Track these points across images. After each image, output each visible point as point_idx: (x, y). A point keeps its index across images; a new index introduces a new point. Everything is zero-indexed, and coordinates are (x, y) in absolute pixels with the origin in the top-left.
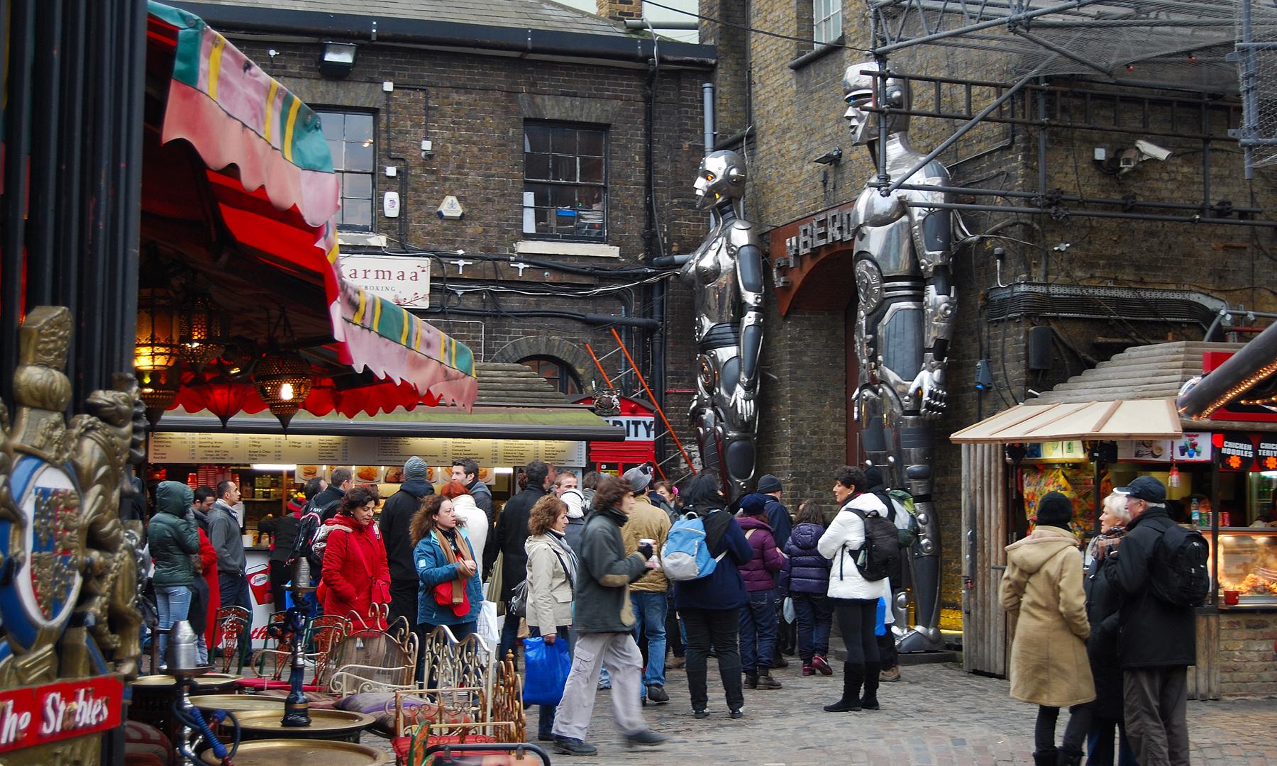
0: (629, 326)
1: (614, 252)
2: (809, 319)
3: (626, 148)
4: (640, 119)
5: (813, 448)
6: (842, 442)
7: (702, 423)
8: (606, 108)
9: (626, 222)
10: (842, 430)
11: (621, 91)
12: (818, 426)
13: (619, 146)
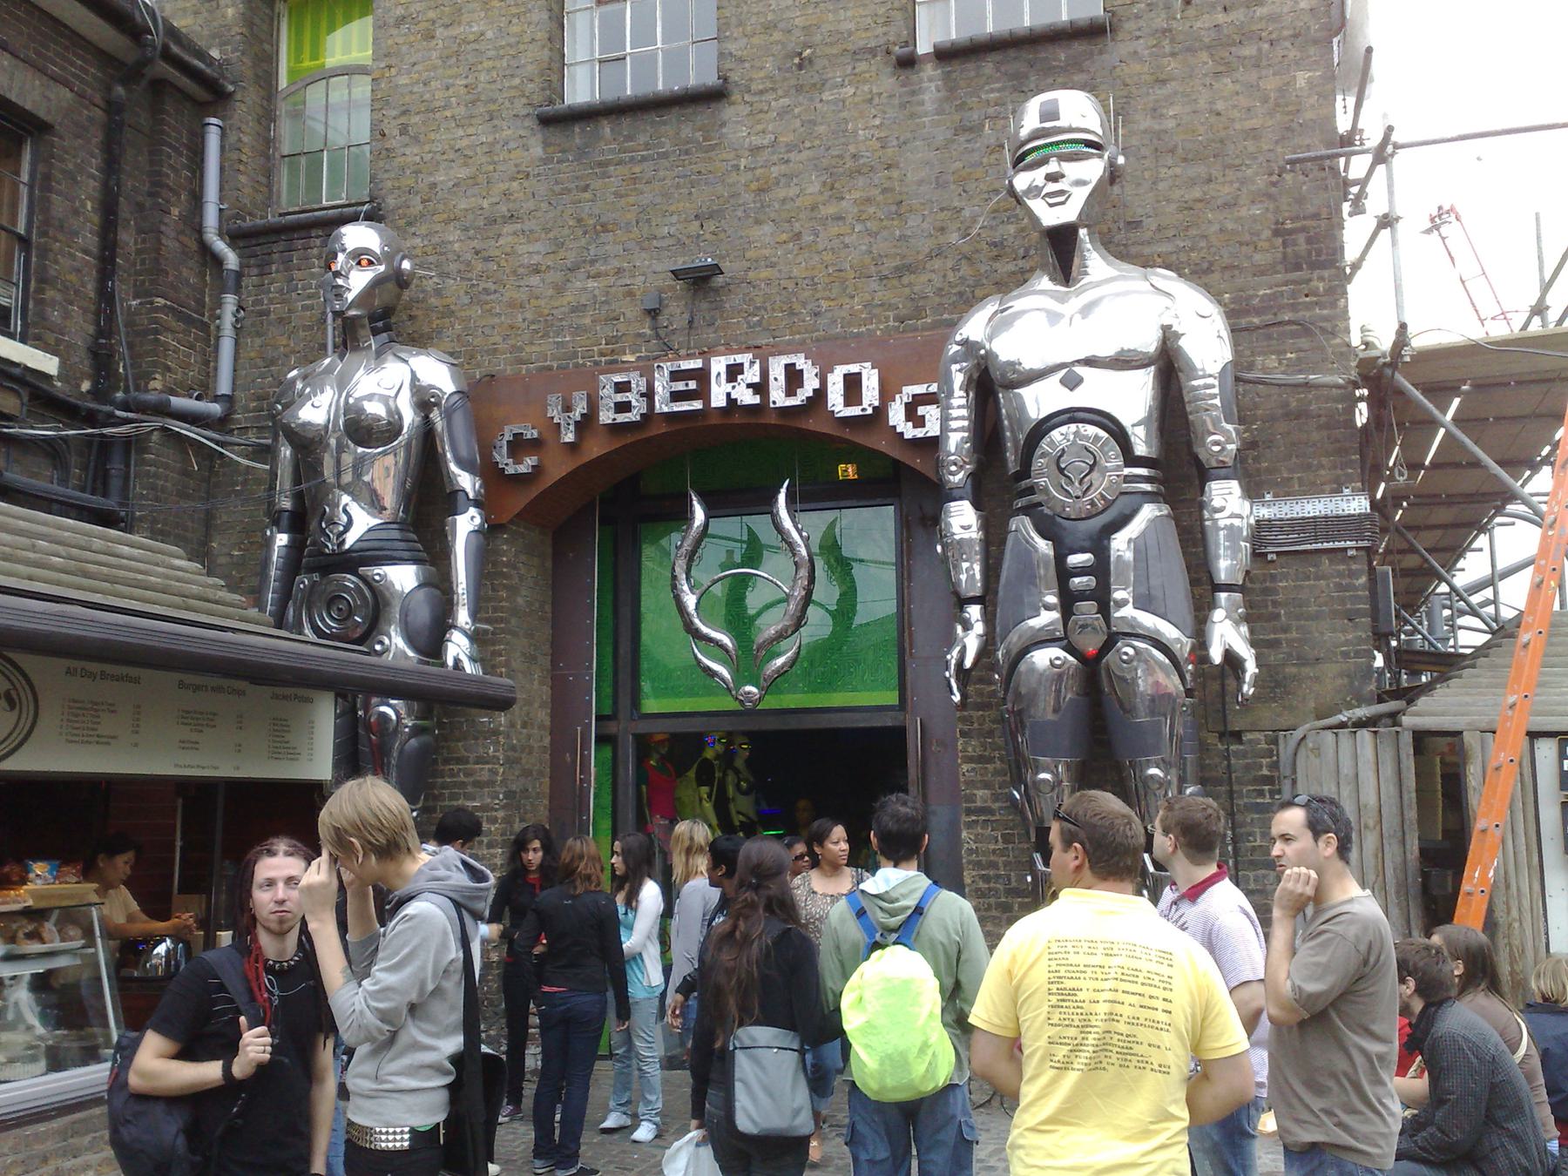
1: (48, 364)
3: (74, 179)
4: (96, 136)
5: (522, 752)
9: (67, 315)
13: (64, 172)
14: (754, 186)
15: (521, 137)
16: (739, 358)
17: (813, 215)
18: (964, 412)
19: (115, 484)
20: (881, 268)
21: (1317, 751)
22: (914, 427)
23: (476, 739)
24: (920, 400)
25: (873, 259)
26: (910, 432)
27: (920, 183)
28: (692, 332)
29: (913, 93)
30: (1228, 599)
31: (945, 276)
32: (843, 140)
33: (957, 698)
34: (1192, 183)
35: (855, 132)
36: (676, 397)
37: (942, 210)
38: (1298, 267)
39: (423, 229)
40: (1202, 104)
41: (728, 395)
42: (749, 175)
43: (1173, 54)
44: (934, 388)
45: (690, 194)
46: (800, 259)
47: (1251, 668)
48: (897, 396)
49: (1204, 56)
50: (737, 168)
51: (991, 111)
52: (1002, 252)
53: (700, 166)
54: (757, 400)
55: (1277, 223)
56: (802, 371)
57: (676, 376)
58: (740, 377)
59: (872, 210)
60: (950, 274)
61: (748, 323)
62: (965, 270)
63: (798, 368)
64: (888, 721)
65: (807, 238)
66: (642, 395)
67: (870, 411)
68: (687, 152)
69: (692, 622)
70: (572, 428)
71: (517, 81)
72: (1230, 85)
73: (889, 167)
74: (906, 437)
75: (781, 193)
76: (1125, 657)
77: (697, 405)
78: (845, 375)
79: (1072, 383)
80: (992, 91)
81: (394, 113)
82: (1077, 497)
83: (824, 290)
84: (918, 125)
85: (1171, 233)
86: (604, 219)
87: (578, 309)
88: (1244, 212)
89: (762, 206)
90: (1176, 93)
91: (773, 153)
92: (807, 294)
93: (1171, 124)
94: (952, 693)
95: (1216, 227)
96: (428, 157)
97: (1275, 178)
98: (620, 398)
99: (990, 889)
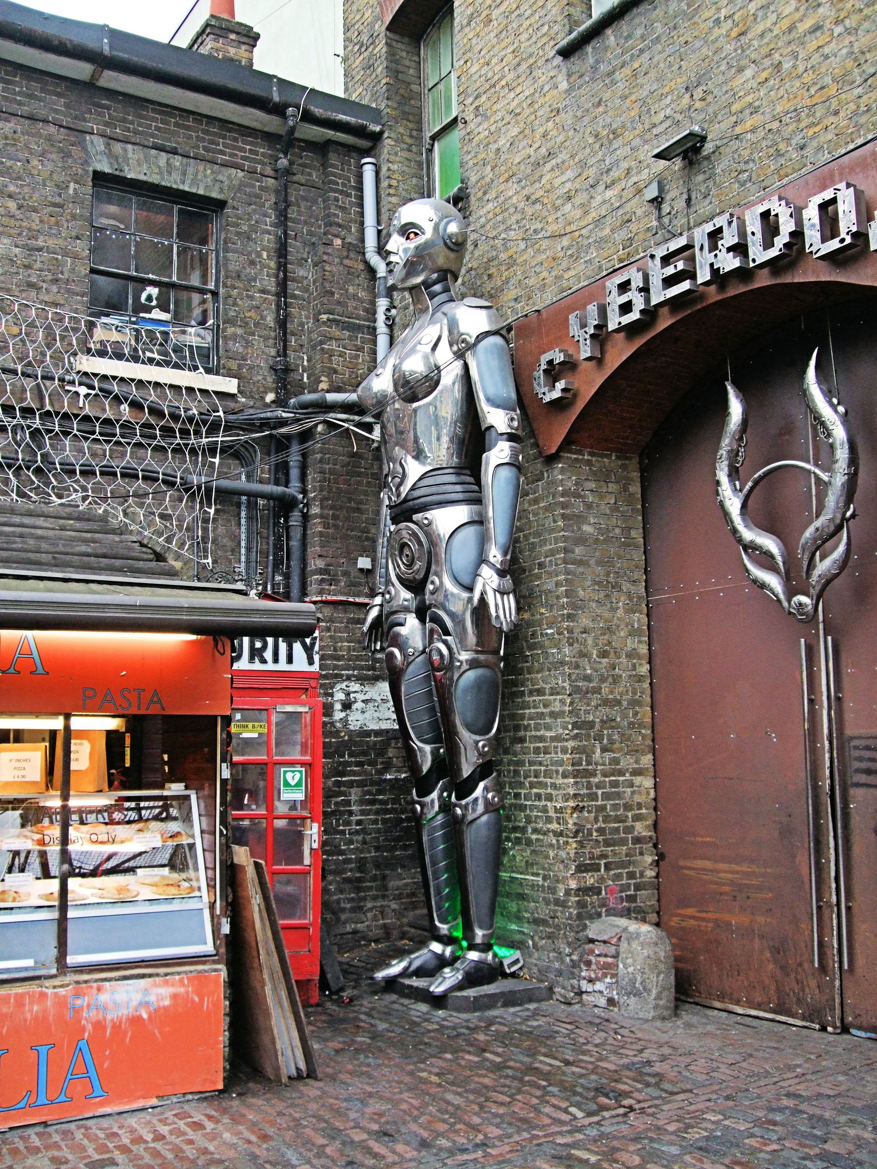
0: (252, 496)
1: (230, 385)
2: (589, 463)
3: (249, 238)
5: (603, 680)
6: (644, 669)
7: (396, 641)
8: (220, 177)
9: (248, 344)
10: (643, 650)
11: (243, 158)
12: (609, 643)
13: (238, 234)
15: (552, 78)
17: (791, 37)
19: (294, 473)
20: (864, 67)
23: (549, 670)
28: (693, 210)
36: (669, 282)
39: (491, 195)
41: (712, 265)
57: (666, 260)
58: (720, 243)
65: (787, 66)
66: (641, 290)
67: (848, 240)
70: (588, 342)
71: (546, 27)
75: (760, 28)
77: (685, 285)
81: (470, 100)
83: (808, 116)
86: (614, 126)
87: (599, 222)
89: (743, 51)
96: (493, 129)
98: (624, 299)
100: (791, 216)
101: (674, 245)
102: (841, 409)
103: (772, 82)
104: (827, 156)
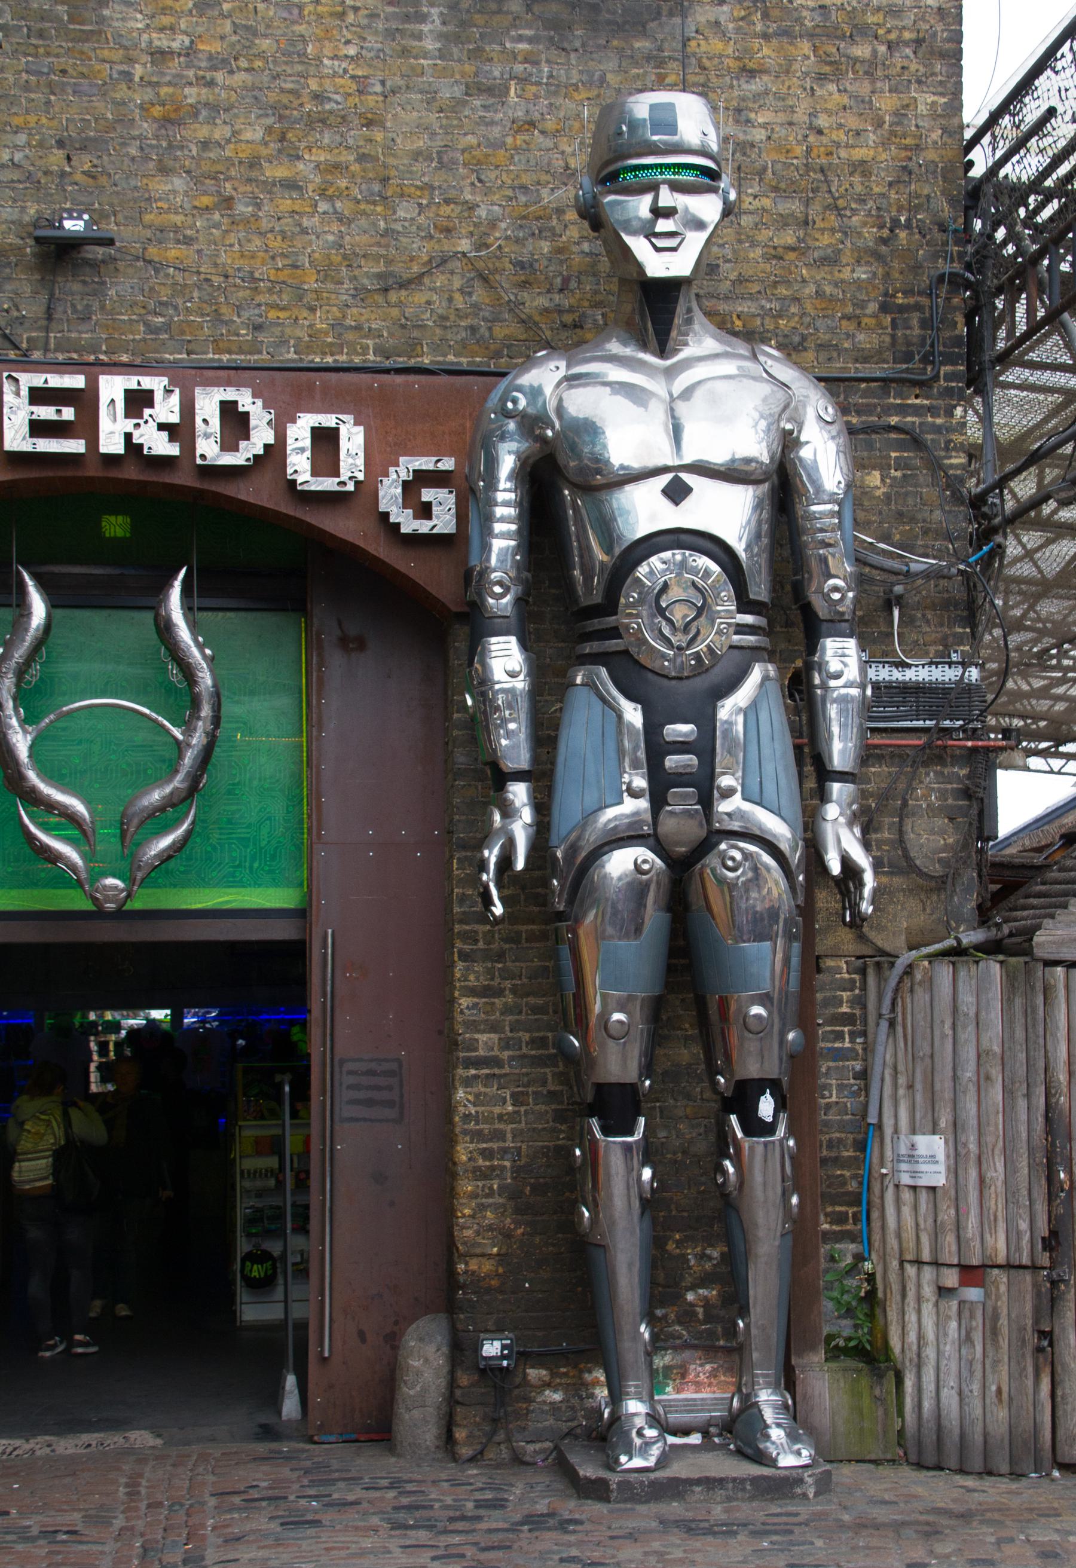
14: (157, 111)
16: (148, 382)
17: (254, 174)
18: (511, 511)
21: (930, 983)
22: (416, 517)
24: (422, 478)
25: (345, 257)
26: (409, 524)
27: (417, 155)
29: (407, 18)
30: (840, 790)
31: (450, 300)
32: (299, 68)
33: (498, 910)
34: (783, 222)
35: (319, 59)
36: (38, 428)
37: (447, 202)
38: (908, 357)
40: (801, 116)
42: (149, 94)
43: (766, 36)
44: (447, 464)
45: (48, 103)
46: (232, 238)
47: (869, 878)
48: (392, 469)
49: (805, 47)
50: (128, 76)
51: (519, 68)
52: (531, 279)
53: (63, 62)
54: (173, 450)
55: (886, 294)
56: (247, 413)
57: (38, 396)
59: (343, 183)
60: (458, 297)
61: (146, 324)
62: (480, 294)
63: (241, 409)
64: (282, 932)
65: (243, 209)
67: (350, 487)
68: (41, 34)
69: (22, 777)
72: (836, 96)
73: (369, 124)
74: (403, 530)
76: (730, 863)
78: (313, 429)
79: (677, 493)
80: (520, 39)
82: (680, 648)
84: (413, 68)
85: (755, 288)
88: (846, 274)
89: (170, 146)
90: (766, 92)
91: (188, 66)
92: (241, 294)
93: (759, 135)
94: (488, 901)
95: (810, 290)
97: (886, 232)
99: (493, 1168)
100: (269, 423)
101: (56, 381)
102: (208, 652)
103: (217, 216)
104: (292, 355)
